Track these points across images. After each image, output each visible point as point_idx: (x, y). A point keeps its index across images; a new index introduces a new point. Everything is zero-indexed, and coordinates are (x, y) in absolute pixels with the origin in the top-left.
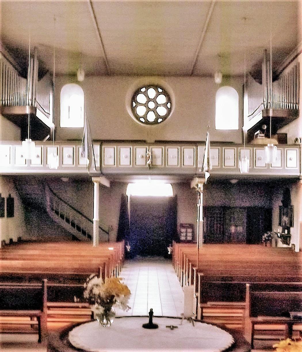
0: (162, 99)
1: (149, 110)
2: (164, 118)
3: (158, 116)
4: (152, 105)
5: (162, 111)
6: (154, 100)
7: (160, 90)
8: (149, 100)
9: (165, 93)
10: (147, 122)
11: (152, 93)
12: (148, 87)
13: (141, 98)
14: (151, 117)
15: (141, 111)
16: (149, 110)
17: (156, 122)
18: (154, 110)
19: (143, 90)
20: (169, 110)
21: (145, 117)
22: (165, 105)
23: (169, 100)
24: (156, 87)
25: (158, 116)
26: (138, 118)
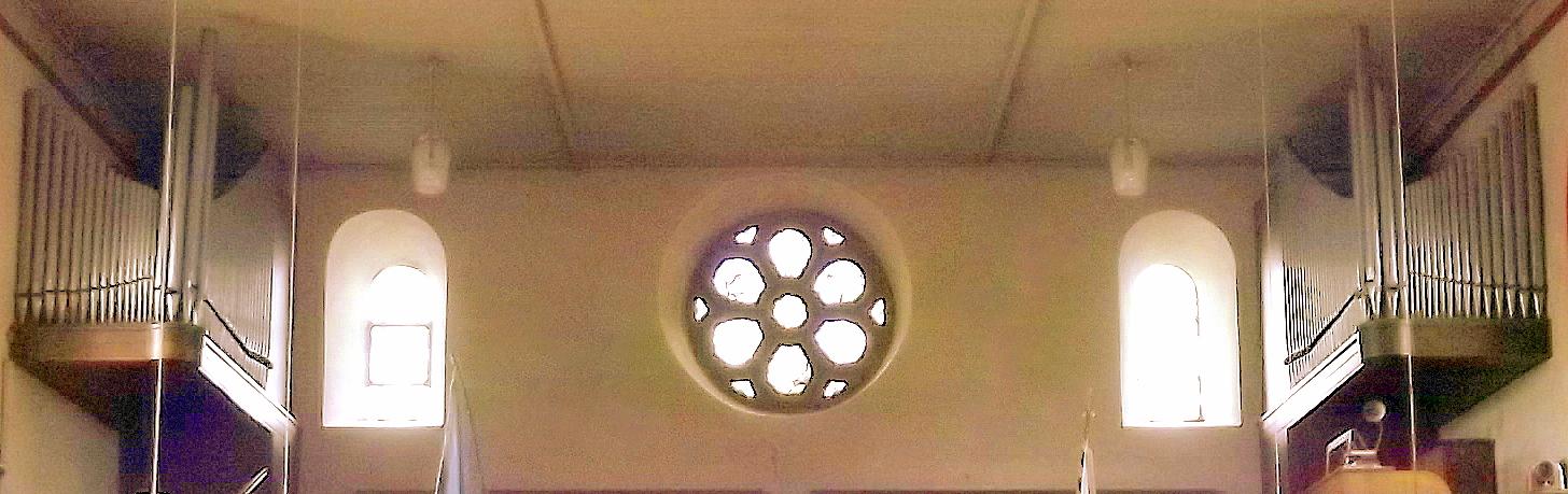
0: (842, 282)
1: (774, 339)
2: (855, 377)
3: (821, 369)
4: (789, 313)
5: (843, 343)
6: (801, 287)
7: (832, 238)
8: (775, 286)
9: (859, 250)
10: (767, 400)
11: (789, 251)
12: (769, 225)
13: (736, 280)
14: (788, 372)
15: (734, 342)
16: (774, 339)
17: (810, 399)
18: (803, 338)
19: (747, 237)
20: (881, 339)
21: (755, 371)
22: (855, 313)
23: (879, 284)
24: (809, 222)
25: (821, 369)
26: (722, 377)
